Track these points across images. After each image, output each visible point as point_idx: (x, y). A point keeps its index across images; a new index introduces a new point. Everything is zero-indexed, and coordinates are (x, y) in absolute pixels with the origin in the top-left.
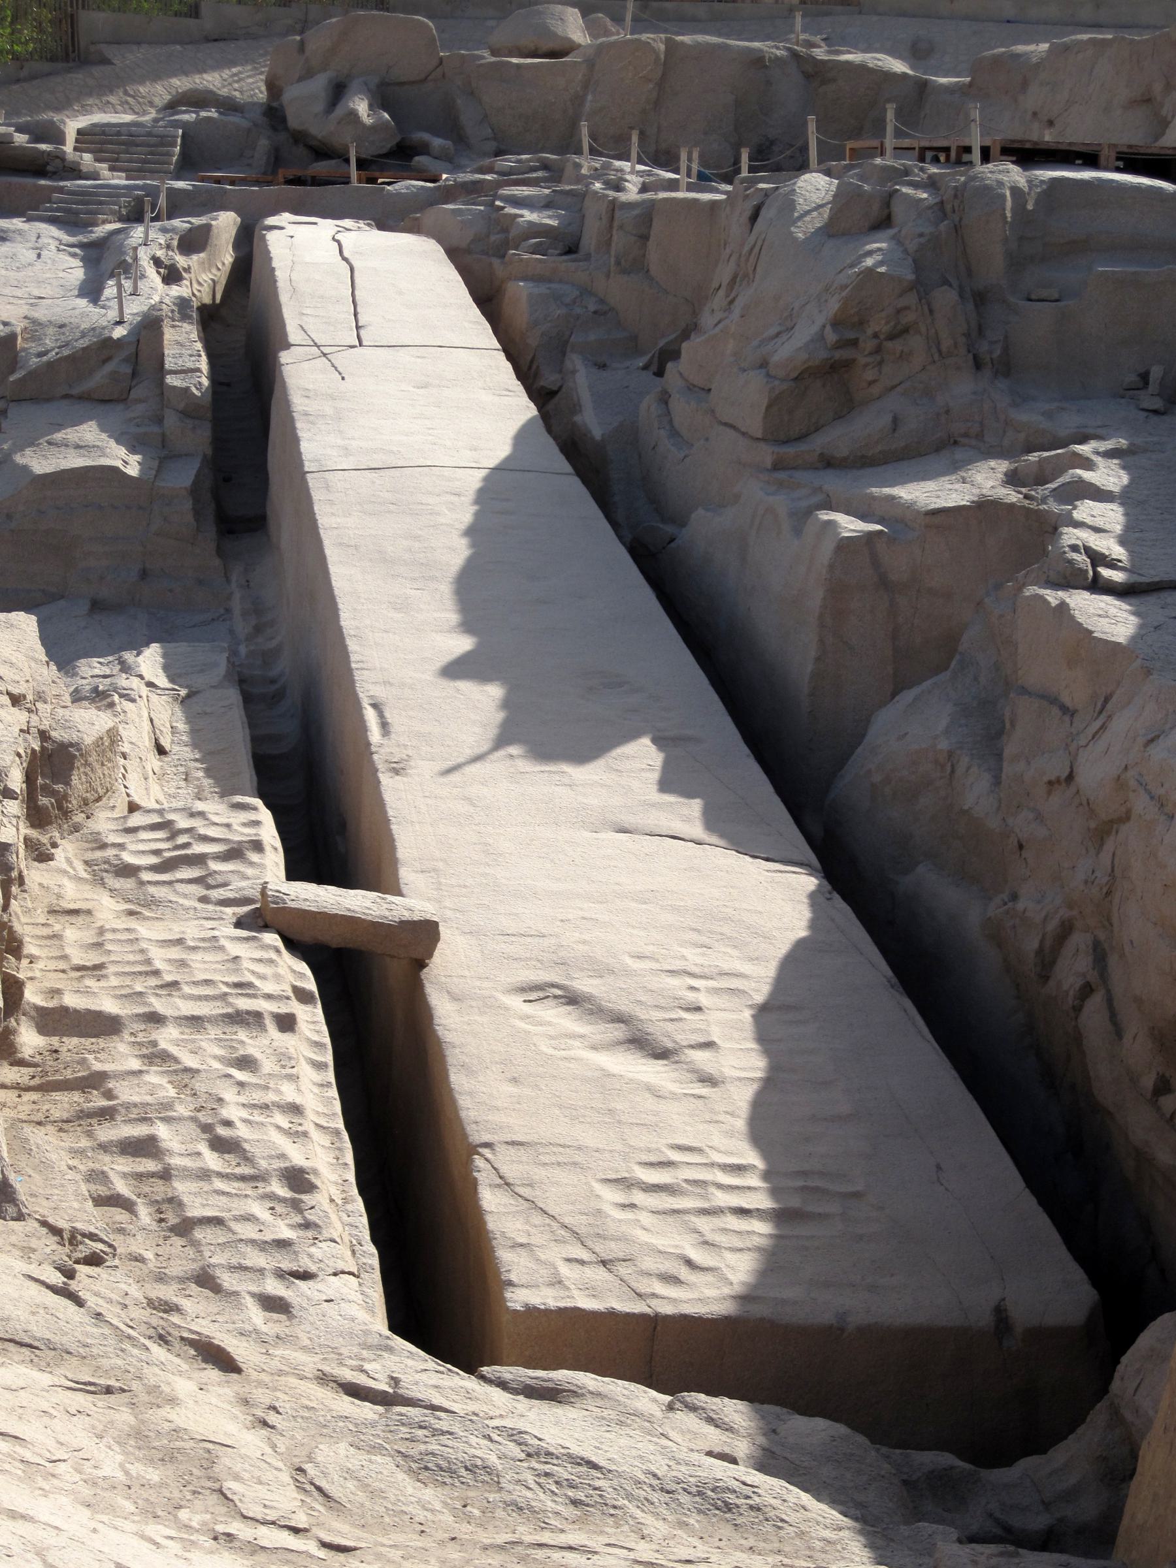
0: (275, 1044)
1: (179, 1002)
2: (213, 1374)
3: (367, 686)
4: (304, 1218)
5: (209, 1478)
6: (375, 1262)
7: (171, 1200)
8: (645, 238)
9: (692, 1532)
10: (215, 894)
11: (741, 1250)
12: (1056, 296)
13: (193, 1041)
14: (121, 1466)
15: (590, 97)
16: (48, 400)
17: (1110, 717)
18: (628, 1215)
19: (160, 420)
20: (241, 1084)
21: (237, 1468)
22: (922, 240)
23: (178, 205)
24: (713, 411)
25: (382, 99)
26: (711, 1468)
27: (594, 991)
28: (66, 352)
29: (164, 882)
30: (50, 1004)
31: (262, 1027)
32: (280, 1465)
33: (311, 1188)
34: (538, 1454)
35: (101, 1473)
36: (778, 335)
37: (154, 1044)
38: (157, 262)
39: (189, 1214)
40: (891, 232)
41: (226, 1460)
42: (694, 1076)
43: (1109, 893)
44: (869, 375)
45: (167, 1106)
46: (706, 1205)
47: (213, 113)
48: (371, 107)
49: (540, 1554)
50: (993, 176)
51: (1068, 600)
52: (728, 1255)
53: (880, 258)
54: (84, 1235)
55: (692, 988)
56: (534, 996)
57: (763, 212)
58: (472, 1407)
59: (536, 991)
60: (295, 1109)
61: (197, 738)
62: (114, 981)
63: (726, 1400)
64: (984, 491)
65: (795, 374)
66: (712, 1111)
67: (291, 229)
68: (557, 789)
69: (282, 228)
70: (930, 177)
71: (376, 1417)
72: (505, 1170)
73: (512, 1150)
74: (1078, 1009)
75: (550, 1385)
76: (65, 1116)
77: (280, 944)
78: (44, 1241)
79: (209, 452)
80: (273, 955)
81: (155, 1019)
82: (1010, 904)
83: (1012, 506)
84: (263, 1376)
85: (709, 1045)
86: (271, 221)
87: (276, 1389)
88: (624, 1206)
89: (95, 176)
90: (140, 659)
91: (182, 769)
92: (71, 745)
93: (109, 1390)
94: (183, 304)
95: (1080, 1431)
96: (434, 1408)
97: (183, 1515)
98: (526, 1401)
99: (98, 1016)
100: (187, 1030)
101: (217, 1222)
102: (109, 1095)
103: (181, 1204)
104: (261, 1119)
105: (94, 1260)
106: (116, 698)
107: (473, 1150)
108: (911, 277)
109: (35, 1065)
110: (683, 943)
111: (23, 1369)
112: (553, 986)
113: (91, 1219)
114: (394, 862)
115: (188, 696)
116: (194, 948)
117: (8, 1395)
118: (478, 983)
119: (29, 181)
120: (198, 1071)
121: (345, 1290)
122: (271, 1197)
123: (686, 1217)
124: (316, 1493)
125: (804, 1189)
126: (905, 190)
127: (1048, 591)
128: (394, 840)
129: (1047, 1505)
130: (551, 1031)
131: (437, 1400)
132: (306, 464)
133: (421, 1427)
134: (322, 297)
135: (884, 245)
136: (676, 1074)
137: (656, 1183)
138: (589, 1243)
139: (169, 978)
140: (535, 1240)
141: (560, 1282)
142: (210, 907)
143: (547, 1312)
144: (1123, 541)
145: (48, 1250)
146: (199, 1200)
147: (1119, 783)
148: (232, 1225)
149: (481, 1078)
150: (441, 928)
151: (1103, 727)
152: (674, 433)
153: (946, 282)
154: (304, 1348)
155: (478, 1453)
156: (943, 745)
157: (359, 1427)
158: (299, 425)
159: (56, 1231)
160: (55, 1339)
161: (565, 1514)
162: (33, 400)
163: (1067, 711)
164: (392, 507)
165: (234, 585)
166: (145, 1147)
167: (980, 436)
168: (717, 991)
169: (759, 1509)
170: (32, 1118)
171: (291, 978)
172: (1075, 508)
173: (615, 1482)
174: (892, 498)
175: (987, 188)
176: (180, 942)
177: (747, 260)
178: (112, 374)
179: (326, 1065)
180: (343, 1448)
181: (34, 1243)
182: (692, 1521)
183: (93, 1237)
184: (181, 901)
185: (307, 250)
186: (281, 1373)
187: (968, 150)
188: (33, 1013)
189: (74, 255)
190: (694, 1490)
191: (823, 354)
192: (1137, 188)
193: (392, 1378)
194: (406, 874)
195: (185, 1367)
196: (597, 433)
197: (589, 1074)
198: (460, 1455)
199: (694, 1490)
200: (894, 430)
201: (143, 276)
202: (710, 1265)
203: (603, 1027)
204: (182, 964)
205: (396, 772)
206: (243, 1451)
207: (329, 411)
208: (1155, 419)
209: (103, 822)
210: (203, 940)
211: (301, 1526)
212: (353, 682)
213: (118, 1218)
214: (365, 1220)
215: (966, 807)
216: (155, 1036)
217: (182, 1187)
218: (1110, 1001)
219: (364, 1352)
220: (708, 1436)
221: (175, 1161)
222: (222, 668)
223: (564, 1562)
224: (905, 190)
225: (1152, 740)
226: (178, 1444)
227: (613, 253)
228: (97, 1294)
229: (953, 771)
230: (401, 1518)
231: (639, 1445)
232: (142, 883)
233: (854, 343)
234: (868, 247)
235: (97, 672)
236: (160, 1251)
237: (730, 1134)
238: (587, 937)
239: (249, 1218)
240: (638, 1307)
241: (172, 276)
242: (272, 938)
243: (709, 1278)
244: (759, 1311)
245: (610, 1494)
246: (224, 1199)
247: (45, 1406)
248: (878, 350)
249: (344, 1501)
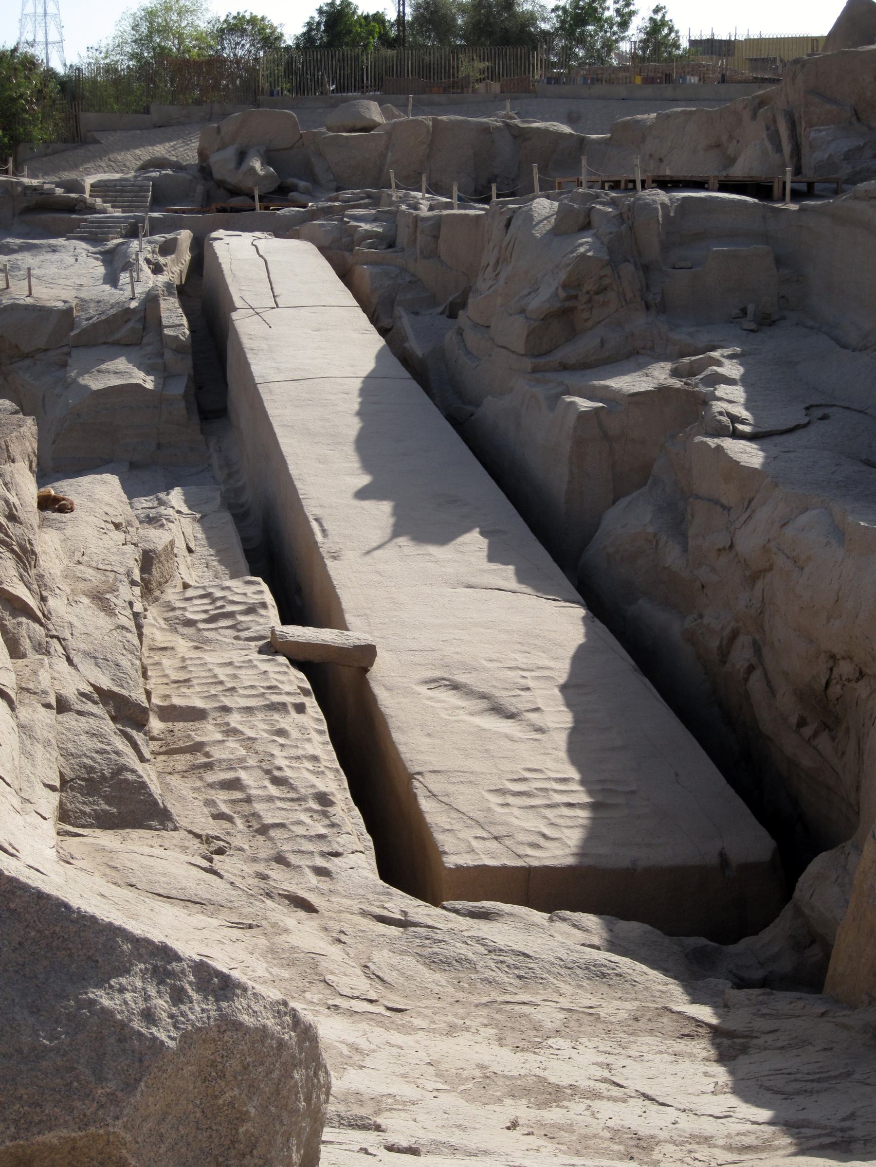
0: (296, 721)
1: (238, 699)
2: (302, 914)
3: (311, 509)
4: (331, 821)
5: (316, 974)
6: (371, 844)
7: (253, 814)
8: (436, 237)
9: (586, 991)
10: (243, 634)
11: (572, 827)
12: (690, 265)
13: (250, 721)
14: (267, 969)
15: (390, 154)
16: (94, 346)
17: (754, 511)
18: (505, 810)
19: (162, 355)
20: (282, 745)
21: (331, 967)
22: (611, 236)
23: (156, 227)
24: (493, 340)
25: (268, 161)
26: (590, 953)
27: (468, 682)
28: (103, 317)
29: (212, 629)
30: (165, 704)
31: (287, 712)
32: (354, 964)
33: (331, 803)
34: (495, 951)
35: (257, 974)
36: (529, 293)
37: (228, 724)
38: (148, 261)
39: (266, 822)
40: (592, 232)
41: (324, 963)
42: (531, 728)
43: (761, 613)
44: (585, 315)
45: (242, 760)
46: (549, 802)
47: (169, 172)
48: (262, 164)
49: (508, 1007)
50: (651, 198)
51: (722, 444)
52: (566, 830)
53: (588, 247)
54: (212, 837)
55: (523, 677)
56: (433, 685)
57: (513, 222)
58: (450, 925)
59: (434, 682)
60: (315, 758)
61: (211, 542)
62: (198, 689)
63: (581, 914)
64: (661, 381)
65: (541, 317)
66: (544, 748)
67: (227, 240)
68: (429, 564)
69: (221, 239)
70: (612, 198)
71: (400, 934)
72: (431, 787)
73: (434, 776)
74: (746, 680)
75: (484, 910)
76: (184, 768)
77: (287, 662)
78: (192, 842)
79: (192, 373)
80: (285, 669)
81: (226, 709)
82: (699, 620)
83: (678, 389)
84: (331, 914)
85: (537, 710)
86: (214, 235)
87: (340, 921)
88: (502, 805)
89: (104, 211)
90: (170, 497)
91: (204, 561)
92: (151, 551)
93: (250, 927)
94: (168, 286)
95: (777, 921)
96: (428, 927)
97: (308, 995)
98: (471, 920)
99: (193, 709)
100: (245, 716)
101: (282, 826)
102: (207, 755)
103: (259, 817)
104: (297, 765)
105: (220, 852)
106: (164, 521)
107: (411, 776)
108: (607, 258)
109: (161, 740)
110: (513, 651)
111: (201, 917)
112: (443, 679)
113: (212, 828)
114: (341, 611)
115: (201, 518)
116: (240, 667)
117: (197, 932)
118: (400, 680)
119: (65, 216)
120: (256, 739)
121: (359, 862)
122: (309, 810)
123: (539, 810)
124: (377, 979)
125: (603, 790)
126: (598, 207)
127: (708, 439)
128: (339, 598)
129: (762, 965)
130: (446, 705)
131: (430, 923)
132: (256, 378)
133: (427, 939)
134: (251, 279)
135: (589, 240)
136: (520, 728)
137: (517, 790)
138: (486, 827)
139: (229, 685)
140: (455, 827)
141: (473, 851)
142: (241, 642)
143: (468, 868)
144: (747, 409)
145: (195, 847)
146: (269, 814)
147: (765, 549)
148: (291, 827)
149: (410, 735)
150: (378, 650)
151: (750, 517)
152: (468, 353)
153: (627, 260)
154: (345, 896)
155: (461, 951)
156: (650, 529)
157: (392, 941)
158: (248, 356)
159: (198, 836)
160: (213, 898)
161: (515, 984)
162: (86, 346)
164: (309, 402)
166: (234, 784)
167: (652, 349)
168: (537, 678)
169: (621, 976)
170: (165, 770)
171: (296, 681)
172: (716, 389)
173: (540, 964)
174: (607, 387)
175: (647, 205)
176: (230, 664)
177: (506, 250)
178: (131, 330)
179: (324, 732)
180: (385, 952)
181: (187, 844)
182: (585, 984)
183: (217, 838)
184: (224, 639)
185: (237, 251)
186: (340, 911)
187: (634, 182)
188: (156, 709)
189: (97, 259)
190: (583, 966)
192: (732, 201)
193: (402, 911)
194: (349, 618)
195: (285, 911)
196: (420, 353)
197: (472, 729)
198: (452, 953)
199: (583, 966)
201: (141, 270)
202: (558, 838)
203: (475, 702)
204: (235, 677)
205: (335, 558)
206: (332, 957)
207: (265, 347)
208: (752, 334)
209: (171, 595)
210: (244, 662)
211: (373, 999)
212: (301, 507)
213: (225, 826)
214: (362, 820)
215: (667, 565)
216: (227, 719)
217: (259, 807)
218: (766, 674)
219: (382, 898)
220: (574, 936)
221: (253, 792)
222: (218, 501)
223: (522, 1011)
224: (598, 207)
225: (784, 525)
226: (295, 955)
227: (418, 247)
228: (227, 871)
229: (657, 545)
230: (426, 992)
231: (549, 943)
232: (199, 630)
233: (576, 297)
234: (580, 241)
235: (144, 505)
236: (252, 844)
237: (557, 760)
238: (458, 650)
239: (300, 823)
240: (519, 863)
241: (157, 269)
242: (282, 659)
243: (556, 844)
244: (589, 861)
245: (538, 972)
246: (283, 812)
247: (219, 938)
248: (589, 301)
249: (393, 983)
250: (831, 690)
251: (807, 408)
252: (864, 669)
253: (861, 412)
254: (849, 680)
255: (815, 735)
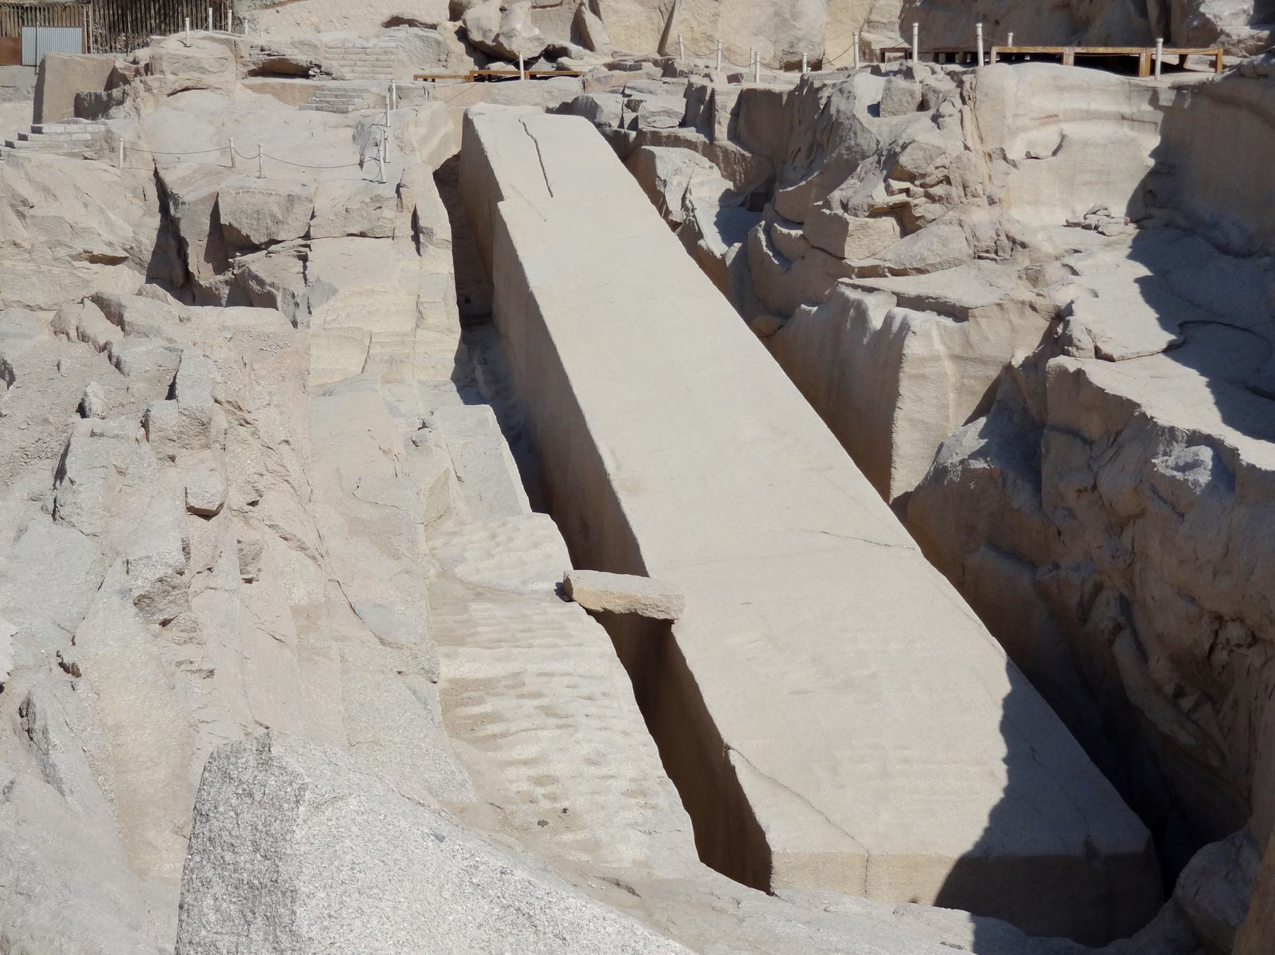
74: (1111, 642)
107: (729, 748)
163: (1088, 442)
165: (475, 362)
250: (1215, 657)
251: (1181, 325)
252: (1258, 634)
253: (1245, 330)
254: (1239, 646)
255: (1196, 707)
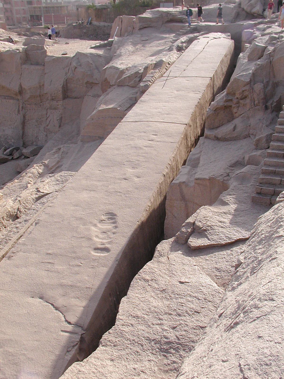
191: (221, 104)
200: (234, 130)
233: (231, 100)
248: (238, 103)
